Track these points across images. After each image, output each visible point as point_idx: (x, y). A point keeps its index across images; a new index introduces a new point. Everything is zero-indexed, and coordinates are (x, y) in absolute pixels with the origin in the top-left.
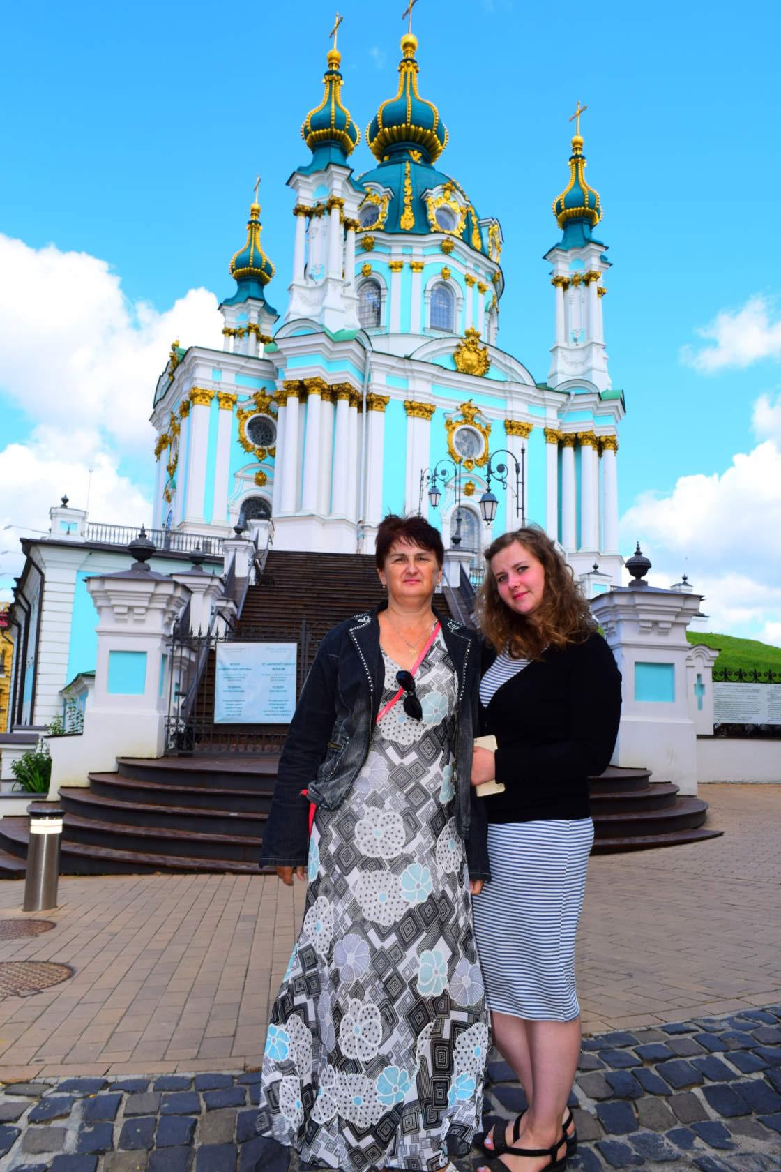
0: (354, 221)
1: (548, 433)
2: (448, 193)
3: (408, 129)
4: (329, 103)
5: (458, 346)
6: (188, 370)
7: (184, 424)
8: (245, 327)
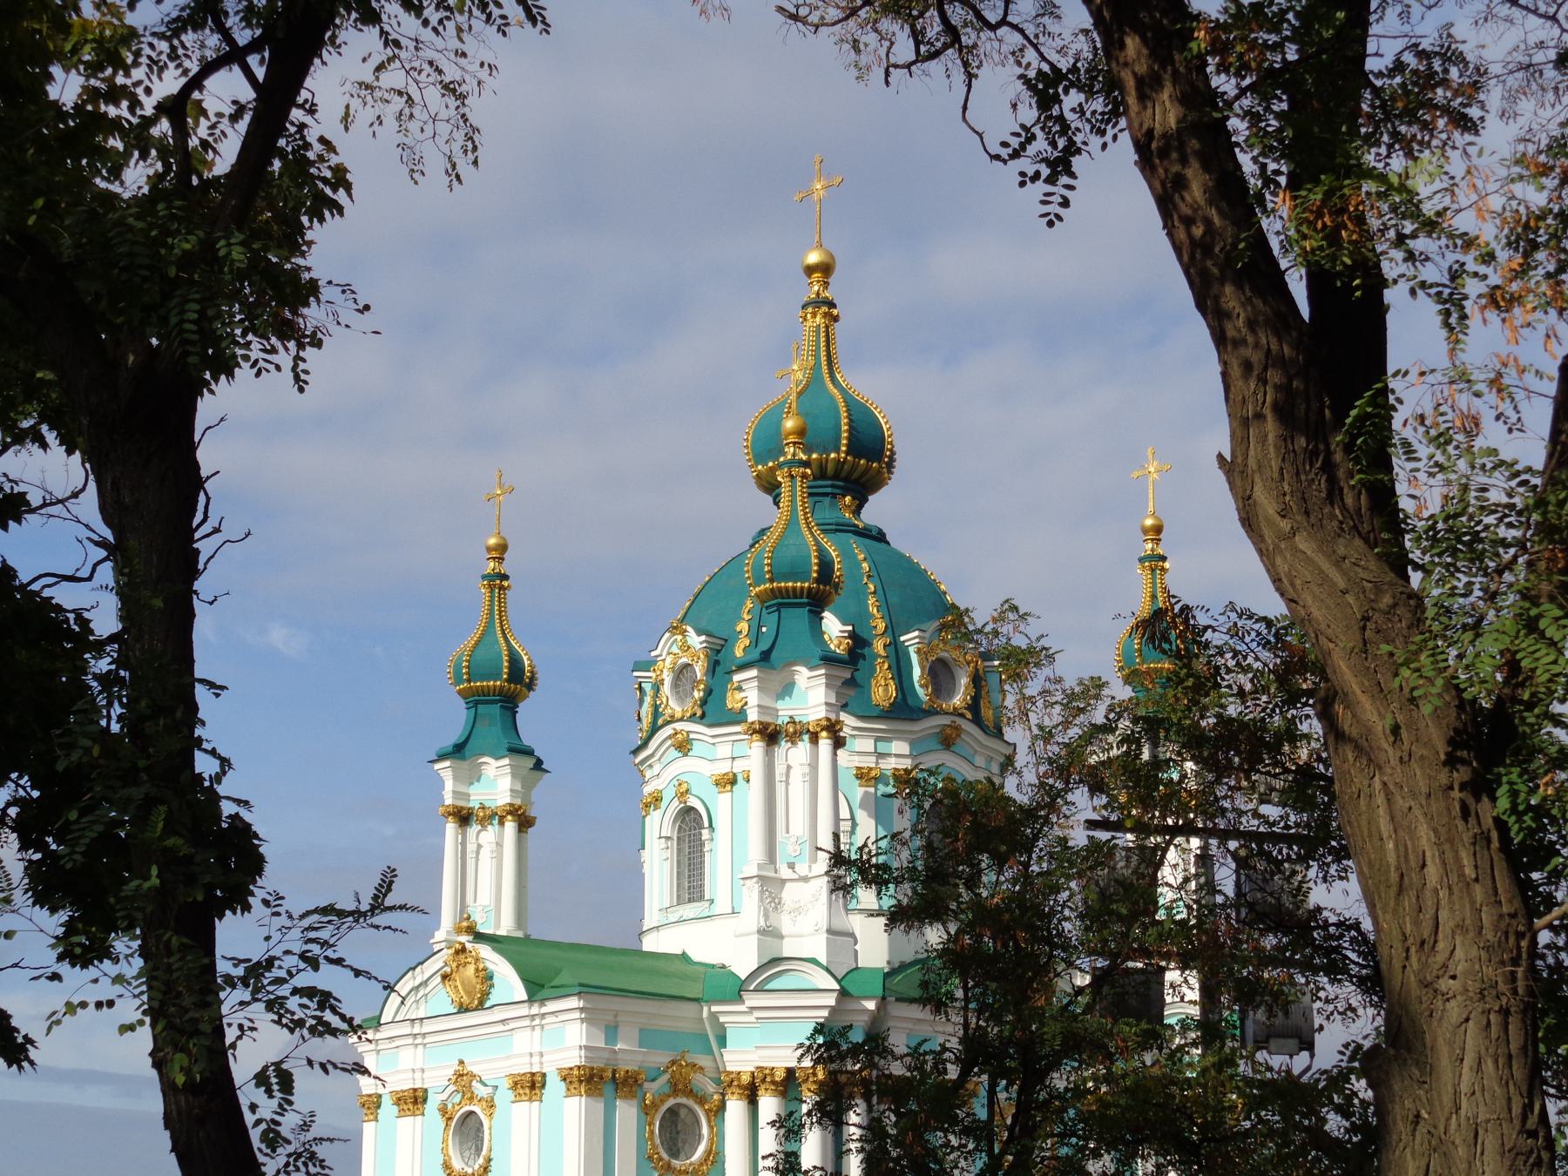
6: (543, 1016)
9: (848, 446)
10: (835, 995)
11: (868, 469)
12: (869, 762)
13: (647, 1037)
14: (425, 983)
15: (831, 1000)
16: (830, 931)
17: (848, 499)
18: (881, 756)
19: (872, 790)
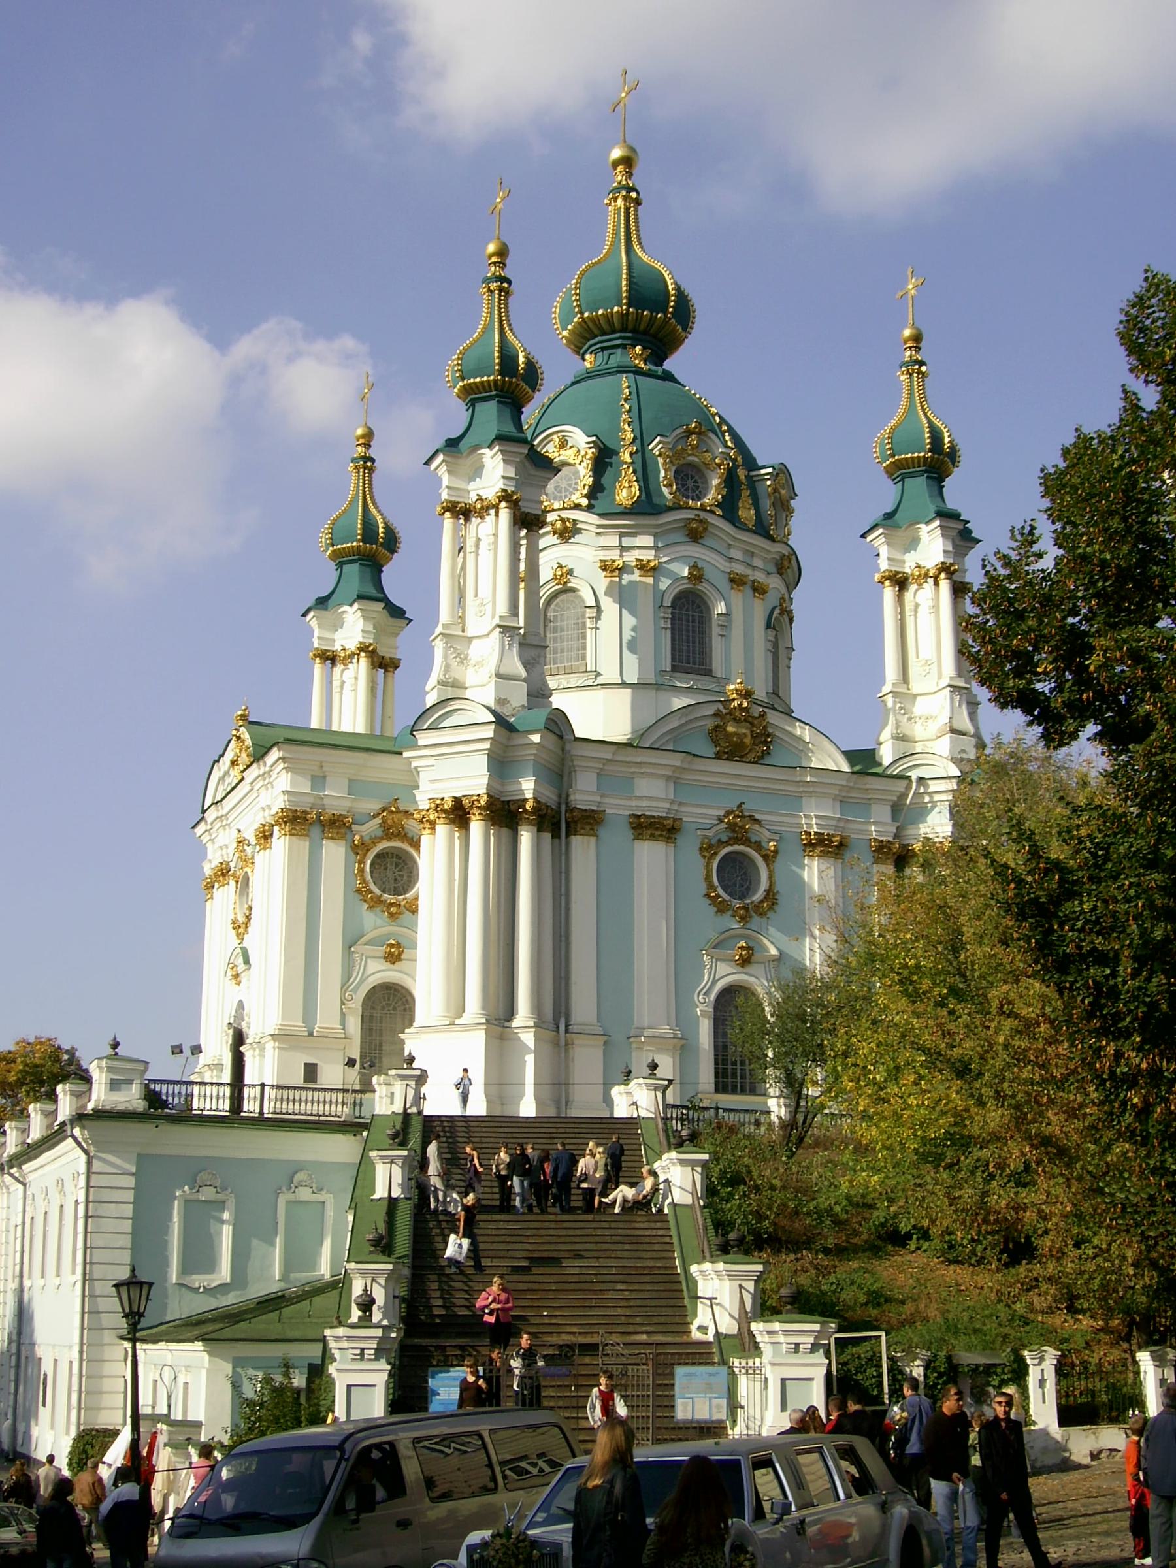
0: (537, 517)
1: (882, 850)
2: (693, 437)
3: (623, 316)
4: (487, 329)
5: (717, 715)
7: (261, 858)
8: (352, 646)
9: (629, 298)
10: (493, 726)
11: (653, 319)
12: (614, 555)
13: (354, 786)
14: (227, 773)
15: (489, 732)
16: (499, 675)
17: (638, 348)
18: (623, 549)
19: (617, 579)
